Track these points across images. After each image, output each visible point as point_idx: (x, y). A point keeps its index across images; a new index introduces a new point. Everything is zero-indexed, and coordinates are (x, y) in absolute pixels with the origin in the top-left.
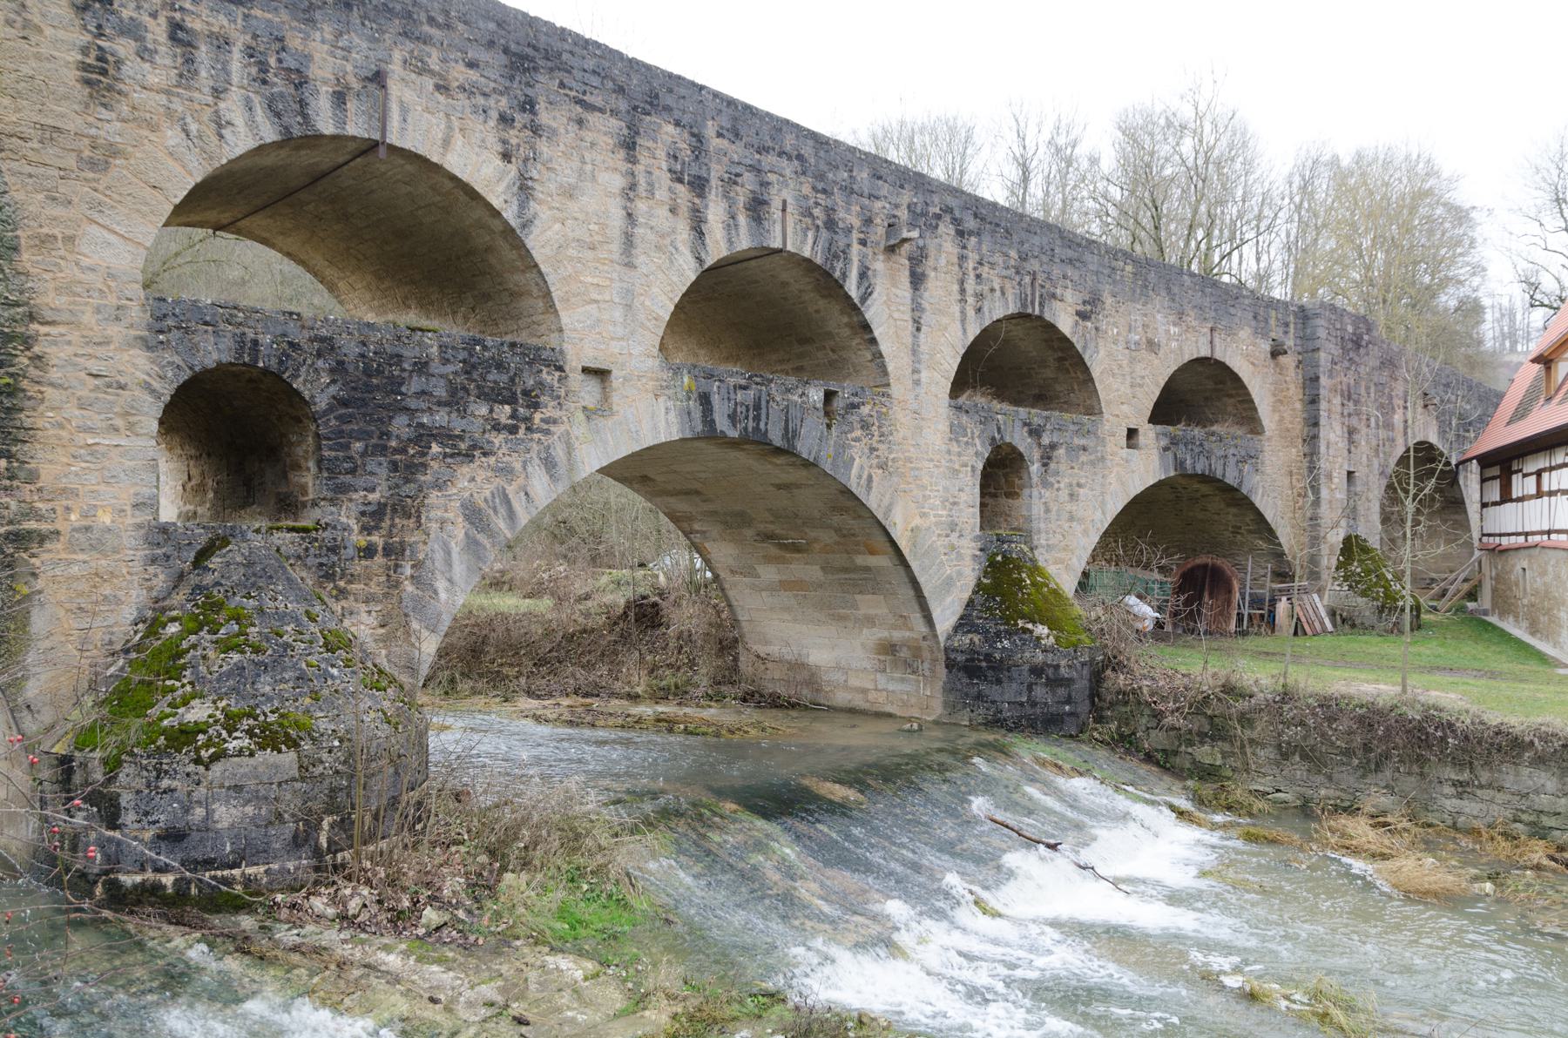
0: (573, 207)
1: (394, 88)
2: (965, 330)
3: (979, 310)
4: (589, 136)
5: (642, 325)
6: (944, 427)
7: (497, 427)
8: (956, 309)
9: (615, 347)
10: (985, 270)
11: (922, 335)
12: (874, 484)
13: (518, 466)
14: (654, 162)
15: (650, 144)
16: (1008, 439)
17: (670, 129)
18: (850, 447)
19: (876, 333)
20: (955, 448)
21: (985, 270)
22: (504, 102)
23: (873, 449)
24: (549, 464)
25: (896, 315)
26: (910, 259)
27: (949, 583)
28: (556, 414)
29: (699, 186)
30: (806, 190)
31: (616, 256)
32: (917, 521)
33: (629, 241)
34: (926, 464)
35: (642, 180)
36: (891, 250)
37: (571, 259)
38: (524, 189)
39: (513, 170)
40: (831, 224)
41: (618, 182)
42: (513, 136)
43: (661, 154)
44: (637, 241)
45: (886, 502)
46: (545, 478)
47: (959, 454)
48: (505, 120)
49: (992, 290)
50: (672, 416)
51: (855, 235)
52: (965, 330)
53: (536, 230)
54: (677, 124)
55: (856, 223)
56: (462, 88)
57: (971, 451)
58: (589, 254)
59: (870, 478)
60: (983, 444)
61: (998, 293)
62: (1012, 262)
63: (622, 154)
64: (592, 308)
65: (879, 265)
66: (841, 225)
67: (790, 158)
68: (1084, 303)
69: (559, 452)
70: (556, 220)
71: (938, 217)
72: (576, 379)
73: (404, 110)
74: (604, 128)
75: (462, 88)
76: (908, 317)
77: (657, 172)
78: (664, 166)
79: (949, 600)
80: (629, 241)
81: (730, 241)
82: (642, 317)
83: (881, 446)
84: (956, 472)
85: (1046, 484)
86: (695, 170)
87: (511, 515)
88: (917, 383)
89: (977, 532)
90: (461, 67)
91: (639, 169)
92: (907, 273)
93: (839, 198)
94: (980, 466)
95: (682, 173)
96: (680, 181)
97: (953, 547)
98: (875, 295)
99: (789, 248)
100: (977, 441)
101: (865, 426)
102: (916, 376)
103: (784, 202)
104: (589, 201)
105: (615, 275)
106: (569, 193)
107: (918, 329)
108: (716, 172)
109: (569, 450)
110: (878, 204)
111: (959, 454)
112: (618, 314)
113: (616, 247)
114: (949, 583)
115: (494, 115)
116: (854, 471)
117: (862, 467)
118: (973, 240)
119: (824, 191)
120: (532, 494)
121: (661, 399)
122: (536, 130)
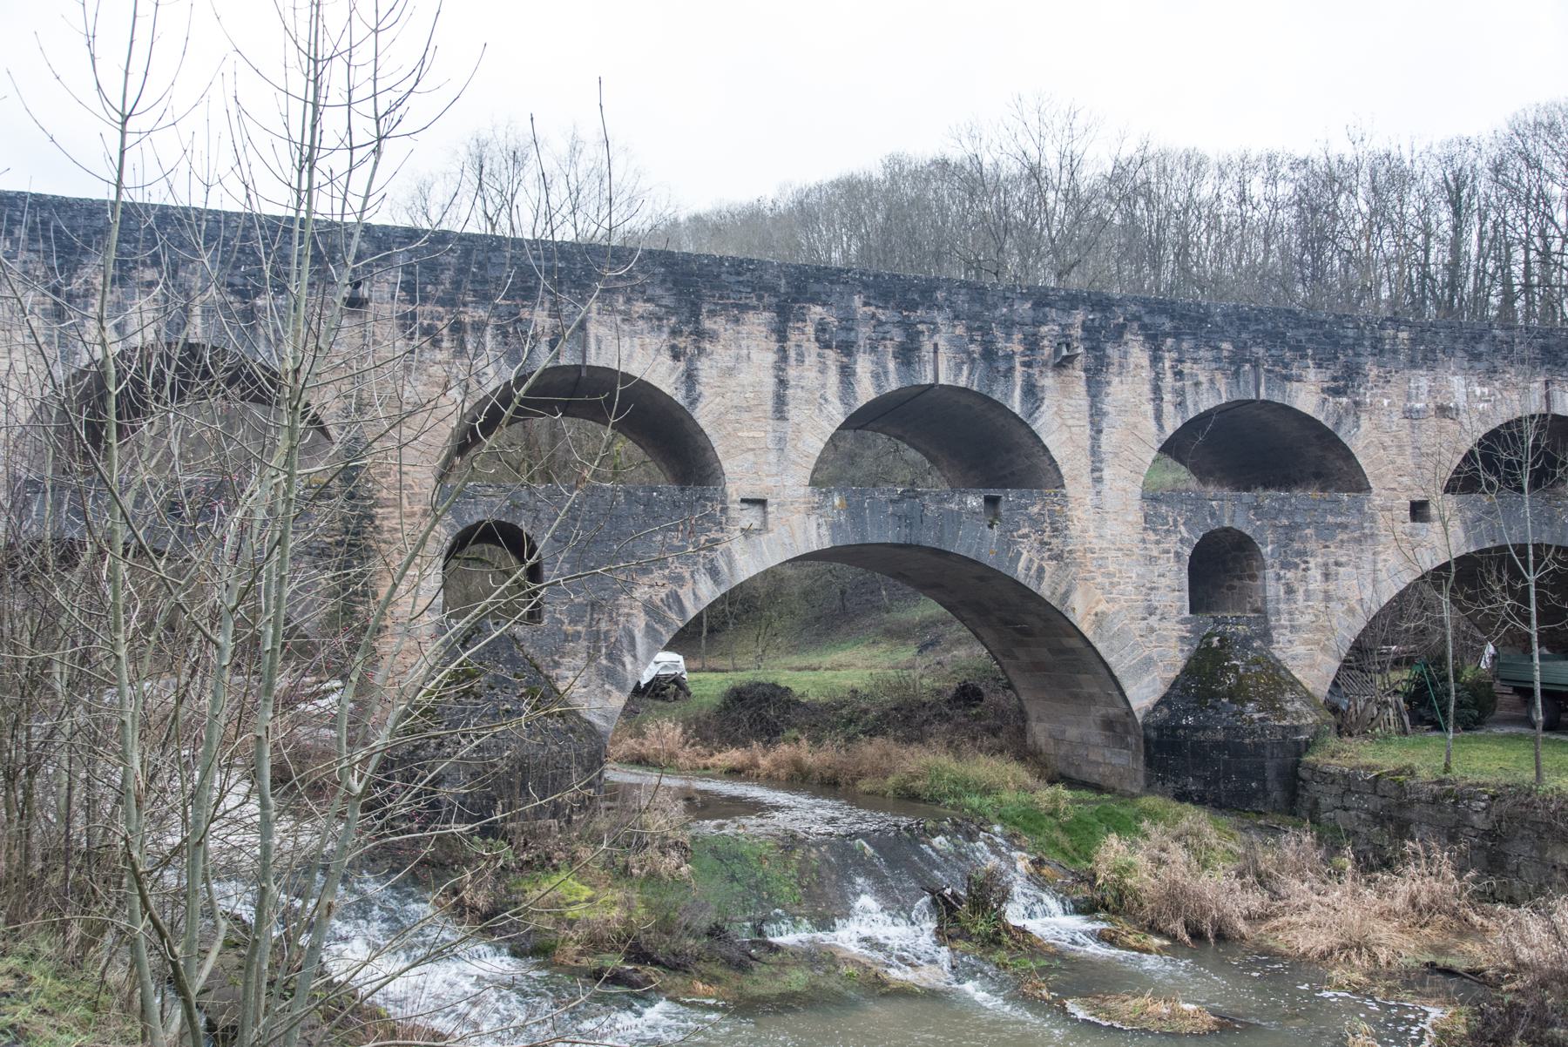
0: (732, 383)
1: (593, 329)
2: (1161, 427)
3: (1180, 405)
4: (744, 329)
5: (794, 463)
6: (1135, 516)
7: (672, 548)
8: (1149, 408)
9: (770, 482)
10: (1187, 367)
11: (1103, 437)
12: (1047, 575)
13: (687, 575)
14: (803, 336)
15: (800, 325)
16: (1227, 524)
17: (818, 309)
18: (1015, 543)
19: (1046, 442)
20: (1152, 537)
21: (1187, 367)
22: (674, 320)
23: (1043, 543)
24: (714, 572)
25: (1070, 422)
26: (1086, 370)
27: (1148, 663)
28: (720, 535)
29: (847, 348)
30: (960, 330)
31: (770, 414)
32: (1101, 608)
33: (780, 402)
34: (1113, 553)
35: (792, 354)
36: (1063, 364)
37: (731, 422)
38: (690, 378)
39: (682, 366)
40: (989, 354)
41: (771, 358)
42: (681, 342)
43: (810, 330)
44: (789, 399)
45: (1062, 589)
46: (710, 582)
47: (1158, 542)
48: (675, 332)
49: (1197, 384)
50: (824, 530)
51: (1018, 360)
52: (1161, 427)
53: (700, 405)
54: (824, 304)
55: (1019, 348)
56: (641, 317)
57: (1174, 538)
58: (746, 416)
59: (1041, 570)
60: (1190, 531)
61: (1205, 386)
62: (1225, 353)
63: (774, 337)
64: (750, 456)
65: (1048, 381)
66: (1001, 353)
67: (940, 308)
68: (1335, 379)
69: (722, 564)
70: (717, 395)
71: (1124, 326)
72: (735, 508)
73: (599, 341)
74: (758, 323)
75: (641, 317)
76: (1086, 422)
77: (806, 344)
78: (812, 338)
79: (1147, 679)
80: (780, 402)
81: (880, 386)
82: (793, 456)
83: (1054, 541)
84: (1151, 560)
85: (1285, 565)
86: (842, 336)
87: (682, 610)
88: (1099, 480)
89: (1187, 613)
90: (640, 304)
91: (790, 344)
92: (1083, 383)
93: (998, 333)
94: (1188, 552)
95: (830, 341)
96: (828, 346)
97: (1152, 630)
98: (1043, 408)
99: (942, 381)
100: (1182, 528)
101: (1034, 522)
102: (1097, 474)
103: (936, 346)
104: (745, 376)
105: (769, 428)
106: (729, 372)
107: (1100, 431)
108: (864, 332)
109: (730, 563)
110: (1044, 329)
111: (1158, 542)
112: (772, 457)
113: (769, 405)
114: (1148, 663)
115: (666, 329)
116: (1022, 564)
117: (1031, 560)
118: (1170, 341)
119: (980, 329)
120: (699, 593)
121: (813, 518)
122: (700, 334)
